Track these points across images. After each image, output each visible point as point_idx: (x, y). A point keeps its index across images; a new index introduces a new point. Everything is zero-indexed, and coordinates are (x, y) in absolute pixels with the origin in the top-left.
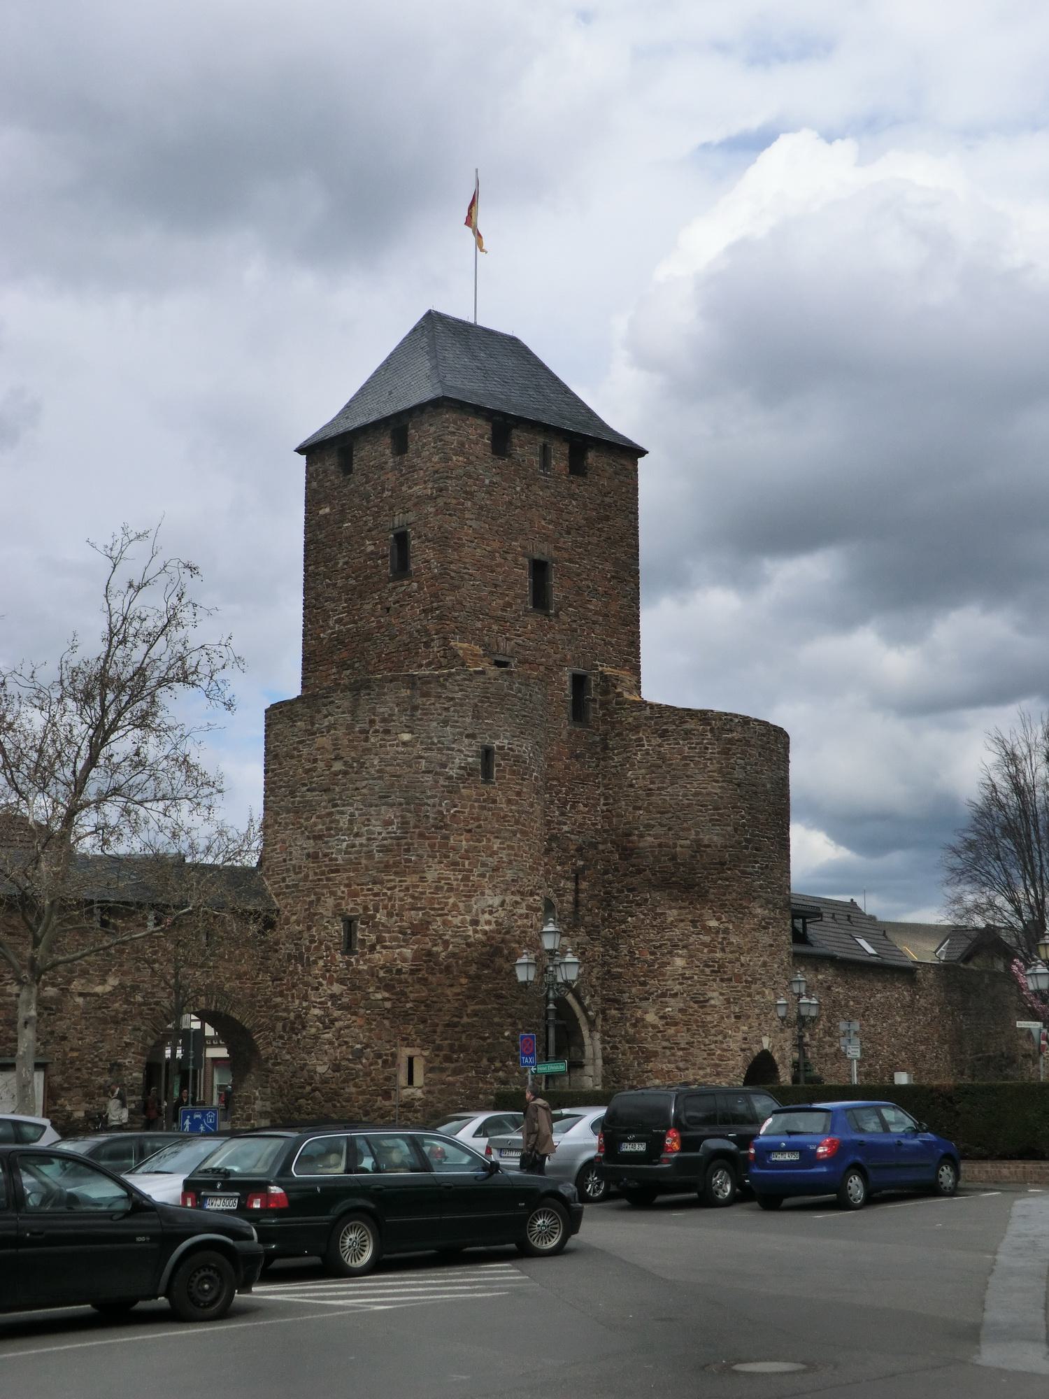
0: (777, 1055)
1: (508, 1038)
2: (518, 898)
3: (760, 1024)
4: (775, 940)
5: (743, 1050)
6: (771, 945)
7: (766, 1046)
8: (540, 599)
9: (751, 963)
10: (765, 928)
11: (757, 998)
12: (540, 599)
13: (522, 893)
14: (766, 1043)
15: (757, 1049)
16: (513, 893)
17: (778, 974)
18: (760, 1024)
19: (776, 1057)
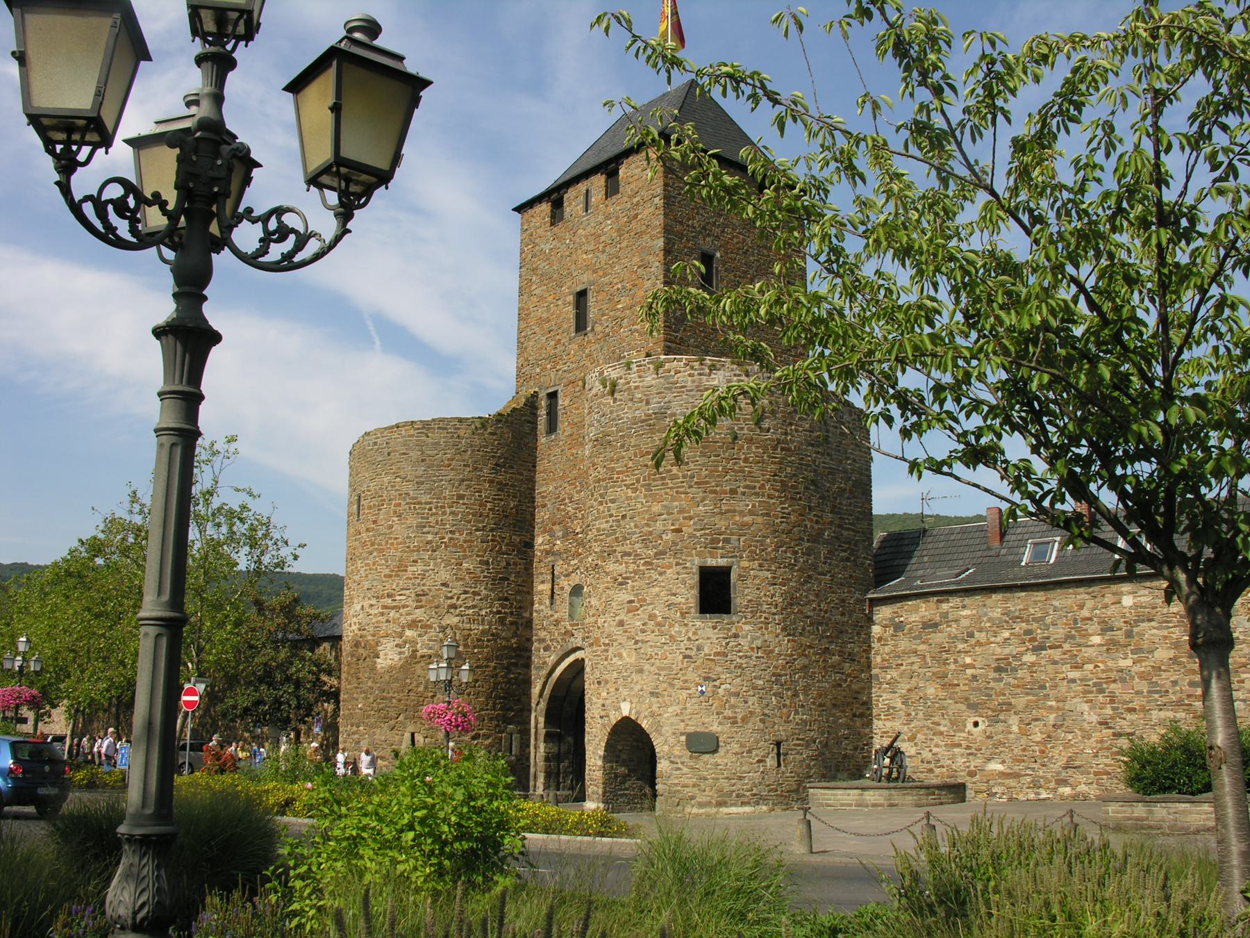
0: (645, 722)
1: (361, 709)
2: (374, 601)
3: (617, 689)
4: (636, 595)
5: (601, 717)
6: (631, 602)
7: (625, 713)
8: (581, 324)
9: (606, 625)
10: (621, 584)
11: (615, 660)
12: (581, 324)
13: (378, 598)
14: (626, 709)
15: (614, 718)
16: (369, 599)
17: (643, 631)
18: (617, 689)
19: (645, 724)
